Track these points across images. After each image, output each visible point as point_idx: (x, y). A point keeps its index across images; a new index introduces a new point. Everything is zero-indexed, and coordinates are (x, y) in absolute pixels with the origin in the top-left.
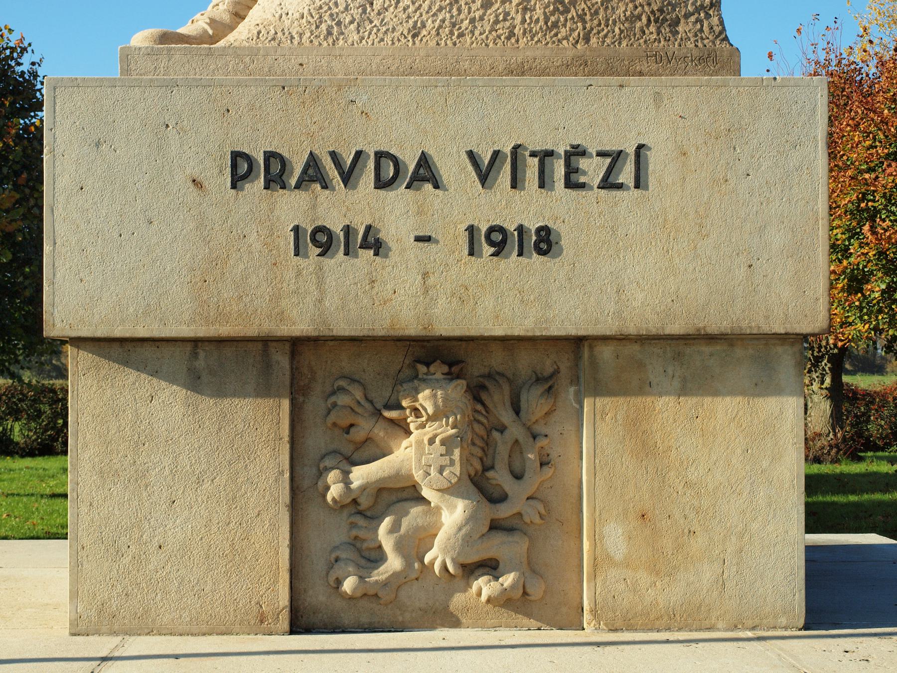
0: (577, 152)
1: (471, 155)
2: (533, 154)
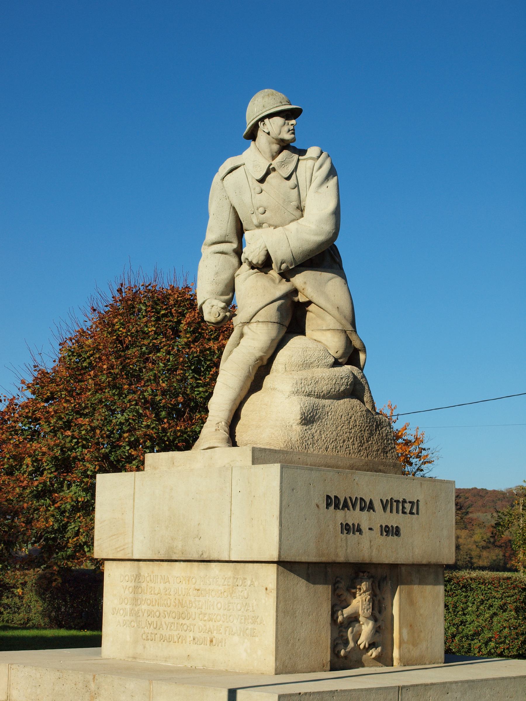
0: (404, 501)
1: (381, 500)
2: (395, 501)
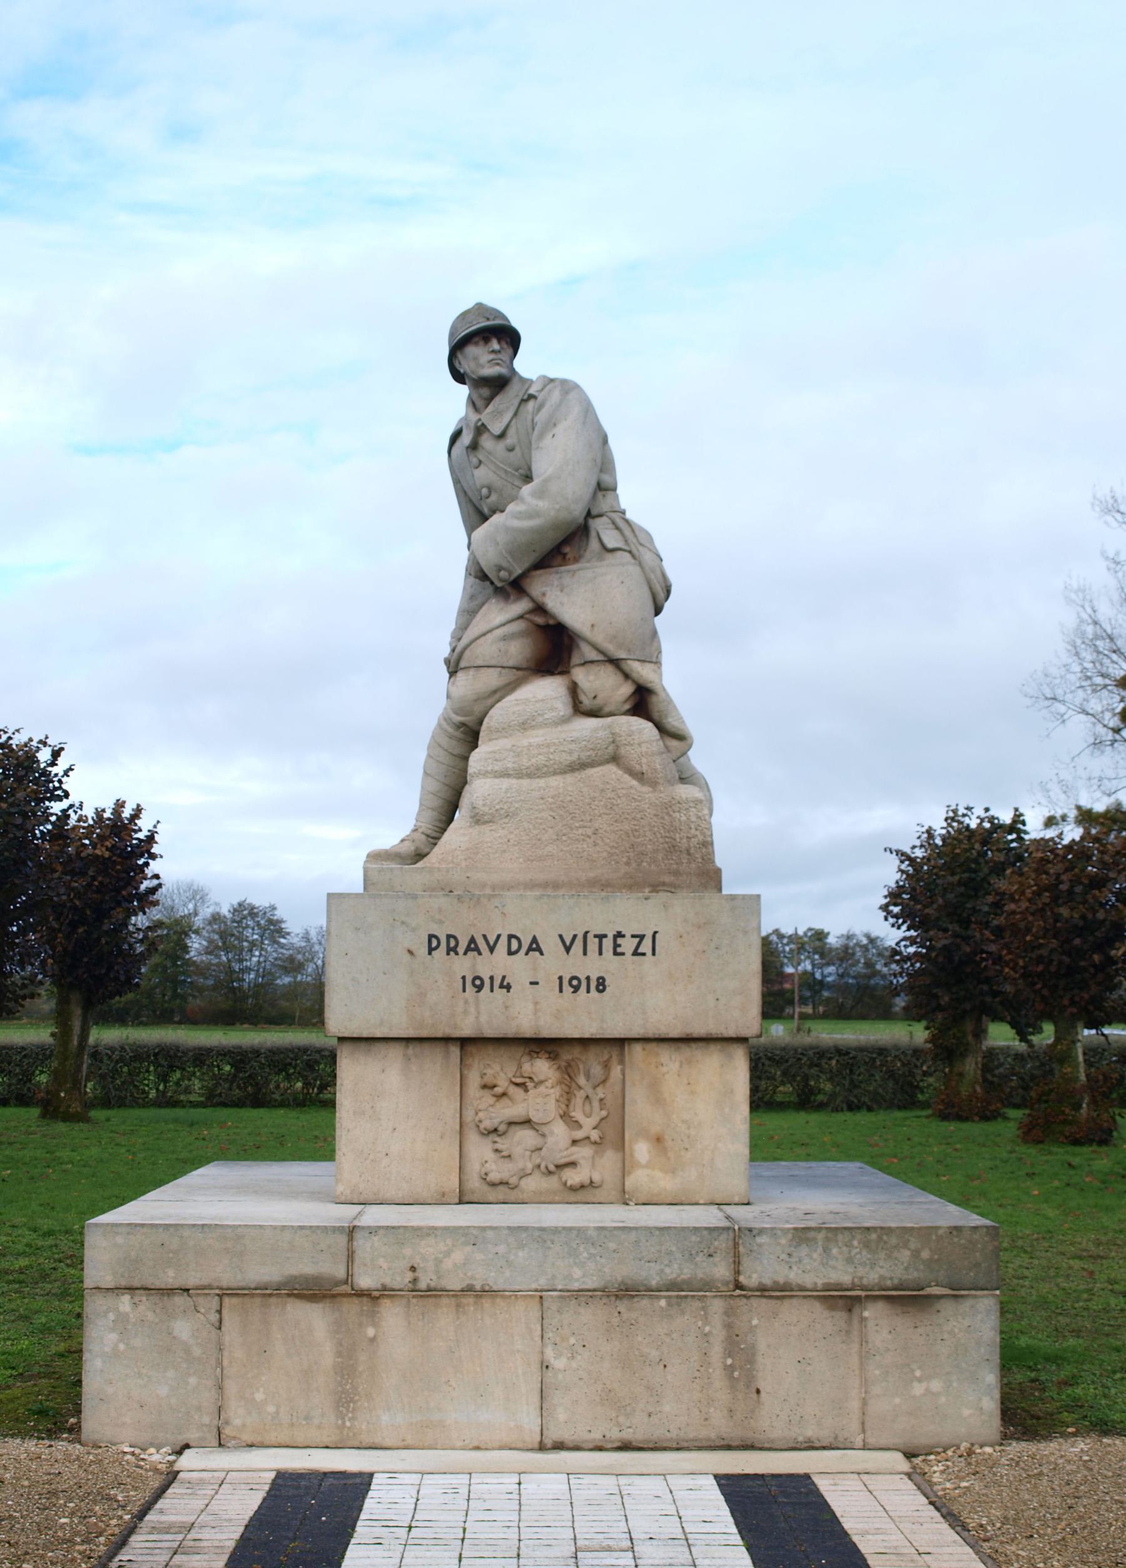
0: (619, 935)
1: (561, 936)
2: (595, 936)
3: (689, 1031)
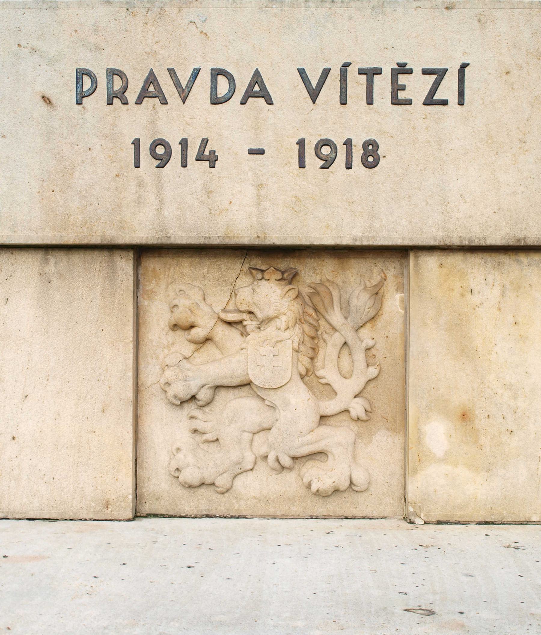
1: (302, 72)
2: (361, 72)
3: (520, 235)
